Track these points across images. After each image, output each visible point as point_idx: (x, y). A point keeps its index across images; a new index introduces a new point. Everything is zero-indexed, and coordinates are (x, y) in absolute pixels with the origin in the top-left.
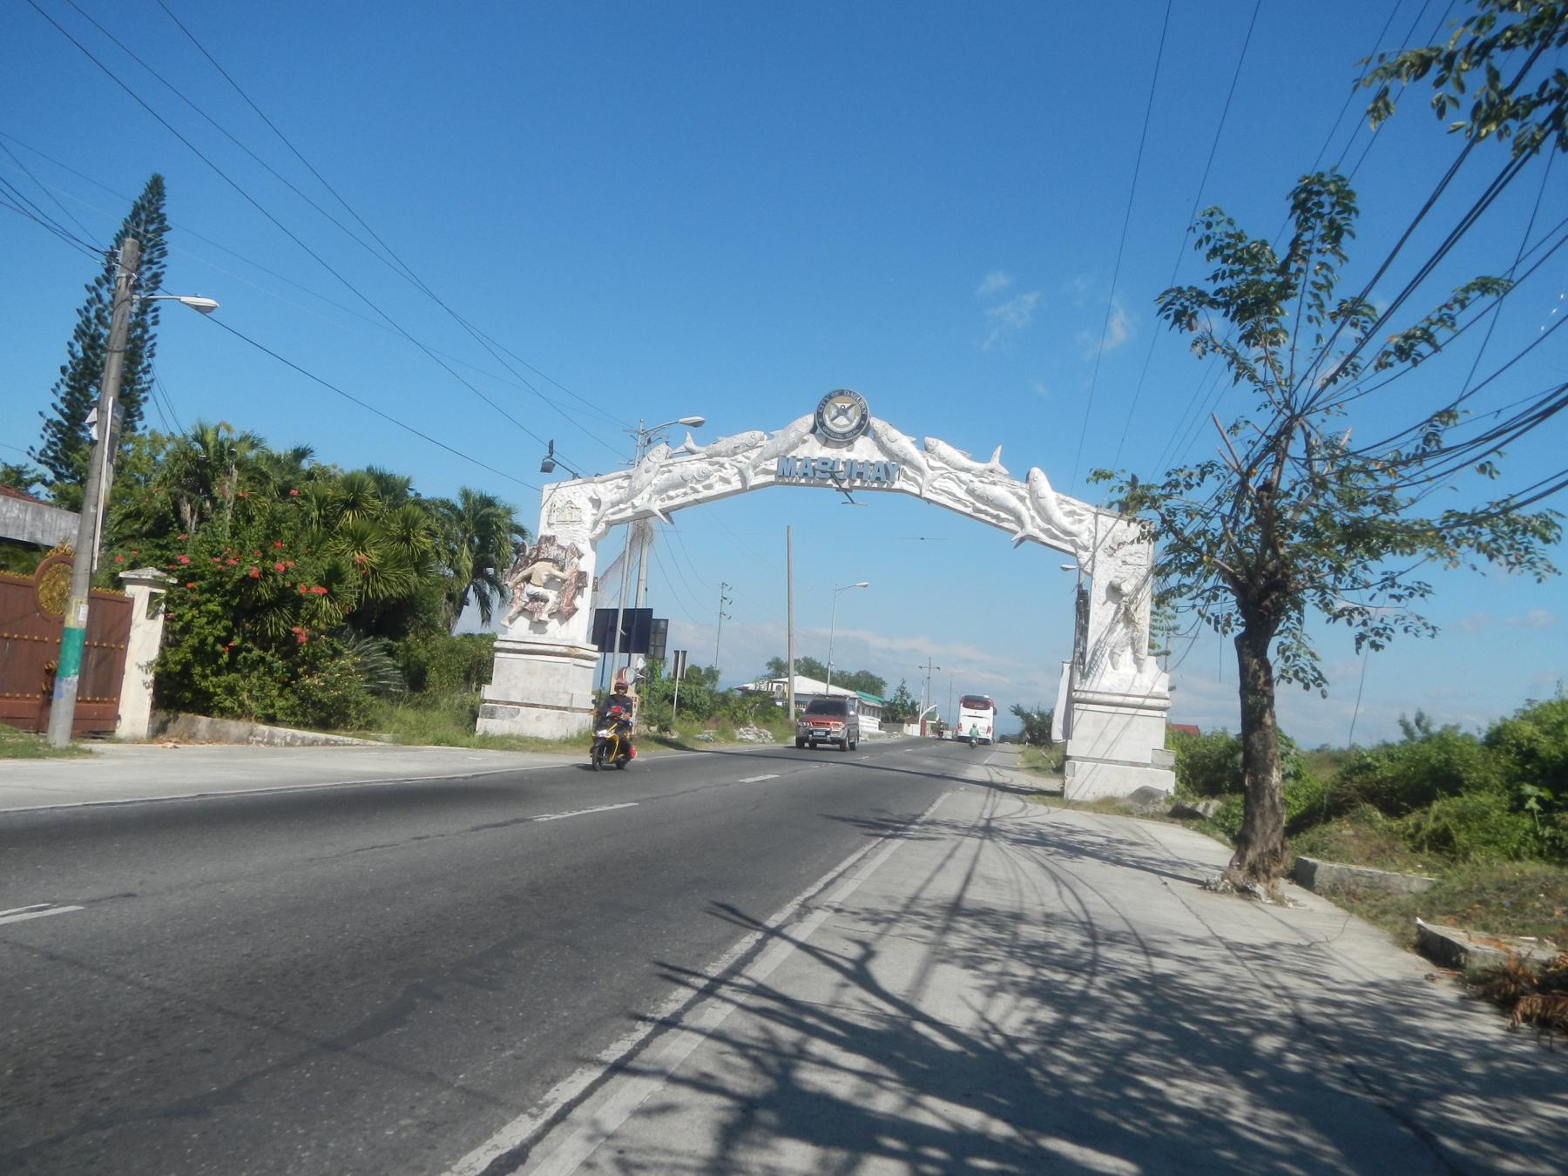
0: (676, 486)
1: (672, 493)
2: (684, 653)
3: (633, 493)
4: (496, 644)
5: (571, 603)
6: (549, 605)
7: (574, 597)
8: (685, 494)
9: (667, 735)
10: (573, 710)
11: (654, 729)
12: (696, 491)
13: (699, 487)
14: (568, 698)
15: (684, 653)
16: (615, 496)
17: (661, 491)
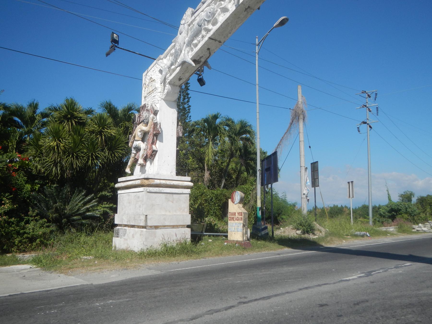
0: (197, 34)
1: (195, 42)
2: (352, 182)
3: (177, 55)
4: (117, 186)
5: (151, 148)
6: (141, 153)
7: (153, 143)
8: (203, 37)
9: (311, 237)
10: (156, 227)
11: (299, 232)
12: (208, 31)
13: (210, 26)
14: (143, 218)
15: (352, 182)
16: (169, 63)
17: (189, 44)
